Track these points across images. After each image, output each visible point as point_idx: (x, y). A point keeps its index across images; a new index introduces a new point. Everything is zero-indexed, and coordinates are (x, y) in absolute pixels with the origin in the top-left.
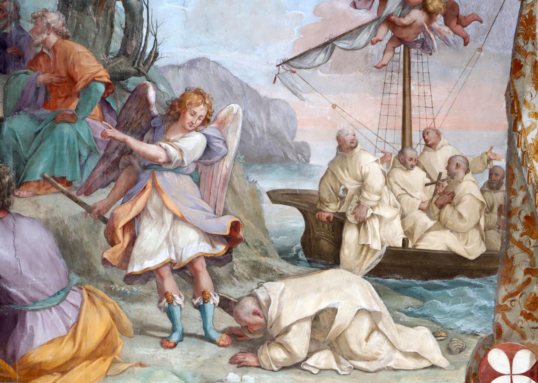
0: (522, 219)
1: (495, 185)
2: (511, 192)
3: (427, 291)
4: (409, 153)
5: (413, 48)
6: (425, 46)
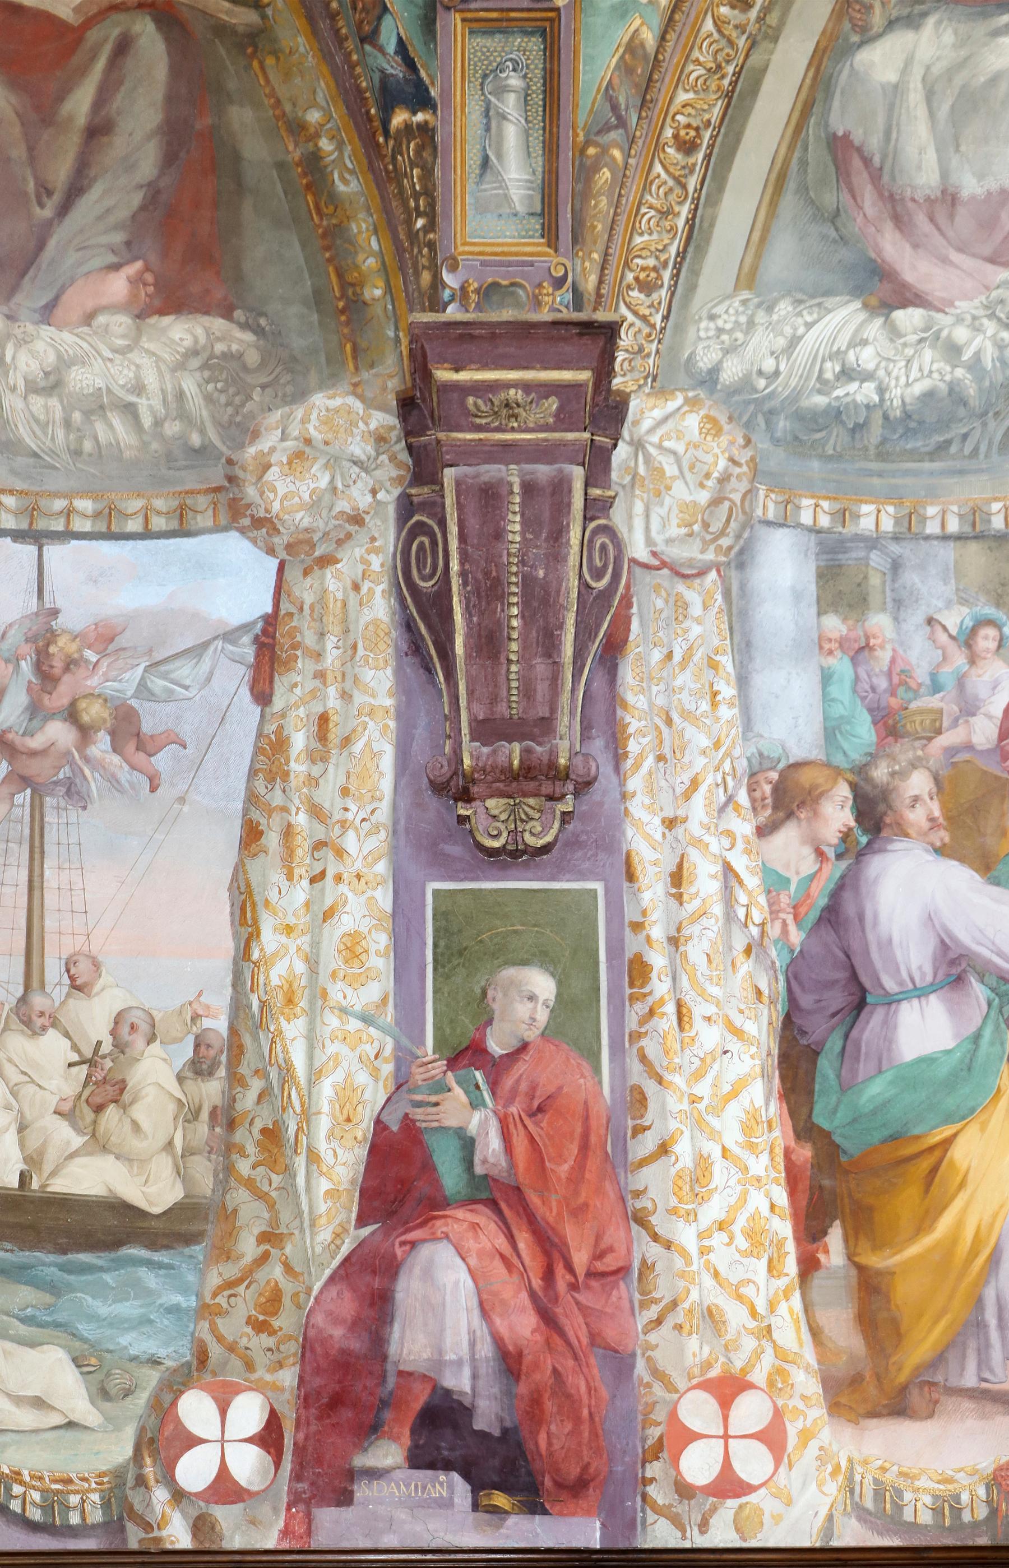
0: (257, 1135)
1: (204, 1067)
2: (235, 1079)
3: (65, 1276)
4: (38, 1001)
5: (48, 795)
6: (74, 792)
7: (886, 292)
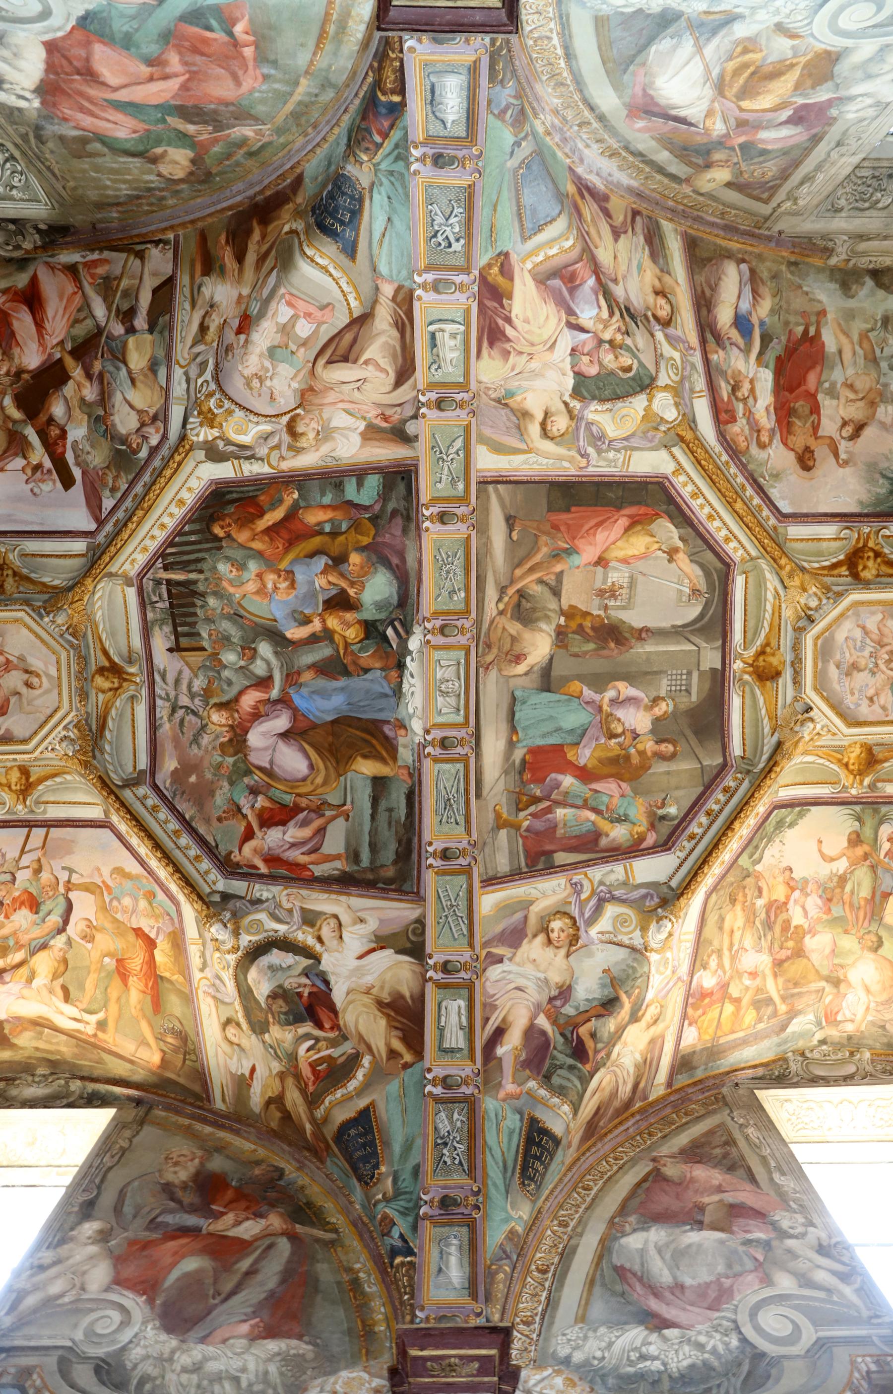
7: (658, 1323)
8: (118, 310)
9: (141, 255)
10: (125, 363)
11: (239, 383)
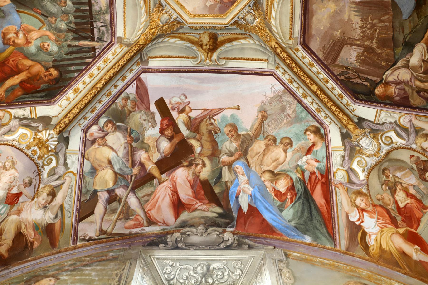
8: (120, 202)
9: (102, 232)
10: (115, 173)
11: (20, 165)
